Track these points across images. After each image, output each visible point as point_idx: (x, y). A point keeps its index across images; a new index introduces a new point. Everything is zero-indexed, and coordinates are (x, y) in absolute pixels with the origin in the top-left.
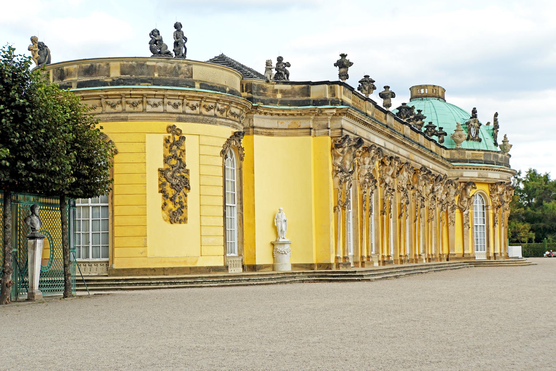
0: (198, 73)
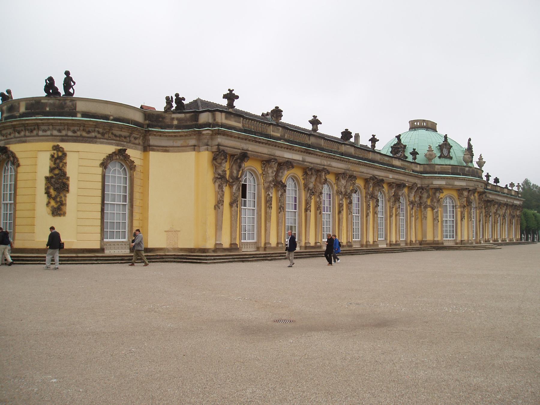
0: (81, 107)
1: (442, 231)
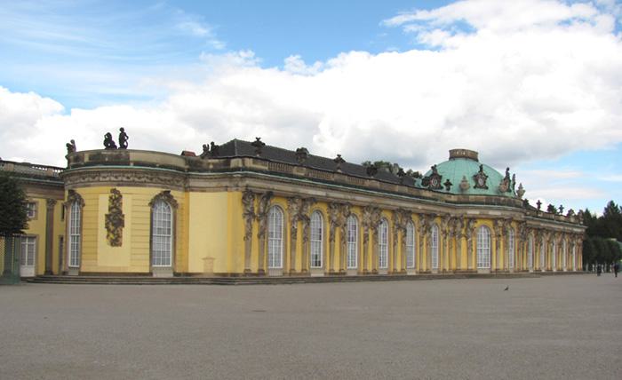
0: (133, 157)
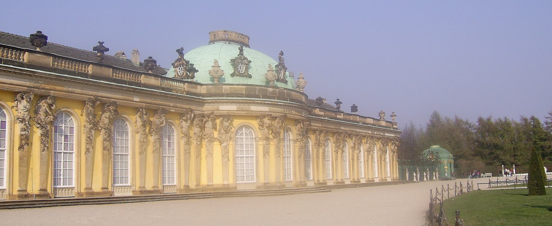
1: (235, 172)
